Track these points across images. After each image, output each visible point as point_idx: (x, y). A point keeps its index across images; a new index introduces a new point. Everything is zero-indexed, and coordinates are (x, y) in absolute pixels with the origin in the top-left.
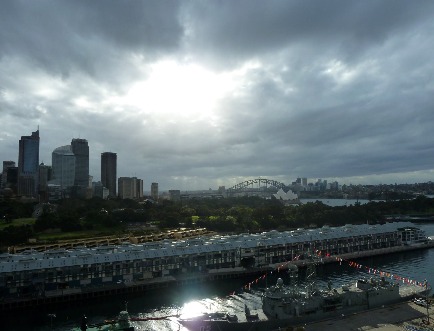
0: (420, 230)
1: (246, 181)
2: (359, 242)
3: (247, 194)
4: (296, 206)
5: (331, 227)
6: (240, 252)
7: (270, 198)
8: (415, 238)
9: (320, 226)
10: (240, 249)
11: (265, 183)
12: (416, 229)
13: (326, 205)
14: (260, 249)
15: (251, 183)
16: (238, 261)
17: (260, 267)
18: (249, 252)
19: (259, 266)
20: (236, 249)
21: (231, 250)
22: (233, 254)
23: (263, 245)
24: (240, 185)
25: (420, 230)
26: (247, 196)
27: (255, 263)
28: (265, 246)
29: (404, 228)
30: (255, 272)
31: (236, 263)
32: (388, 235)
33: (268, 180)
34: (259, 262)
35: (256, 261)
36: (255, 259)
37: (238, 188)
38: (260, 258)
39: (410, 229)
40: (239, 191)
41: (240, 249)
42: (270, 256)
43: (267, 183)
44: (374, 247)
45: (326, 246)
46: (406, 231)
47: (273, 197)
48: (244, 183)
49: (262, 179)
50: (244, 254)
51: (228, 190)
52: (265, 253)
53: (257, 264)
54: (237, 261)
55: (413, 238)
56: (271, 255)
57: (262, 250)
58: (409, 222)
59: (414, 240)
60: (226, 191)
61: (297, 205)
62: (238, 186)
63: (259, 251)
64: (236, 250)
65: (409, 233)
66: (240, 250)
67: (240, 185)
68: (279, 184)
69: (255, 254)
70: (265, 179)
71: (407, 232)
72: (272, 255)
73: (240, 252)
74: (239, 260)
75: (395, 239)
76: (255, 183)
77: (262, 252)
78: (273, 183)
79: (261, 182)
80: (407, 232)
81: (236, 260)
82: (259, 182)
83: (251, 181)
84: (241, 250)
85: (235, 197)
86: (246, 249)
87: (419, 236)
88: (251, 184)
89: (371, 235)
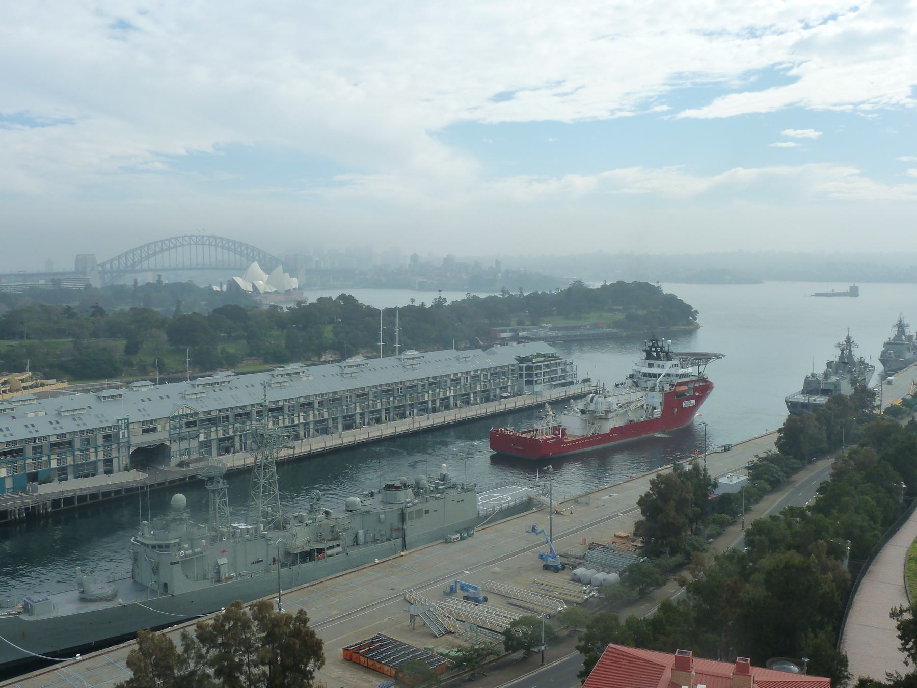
0: (562, 359)
1: (159, 241)
2: (430, 392)
3: (160, 276)
4: (288, 309)
5: (368, 358)
6: (126, 431)
7: (225, 288)
8: (552, 378)
9: (343, 358)
10: (129, 424)
11: (213, 245)
12: (556, 357)
13: (364, 305)
14: (183, 421)
15: (172, 245)
16: (121, 458)
17: (184, 468)
18: (154, 430)
19: (181, 464)
20: (114, 426)
21: (99, 429)
22: (107, 438)
23: (192, 412)
24: (141, 251)
25: (562, 359)
26: (159, 282)
27: (169, 457)
28: (196, 414)
29: (532, 355)
30: (170, 482)
31: (115, 463)
32: (495, 373)
33: (219, 238)
34: (182, 453)
35: (172, 454)
36: (170, 449)
37: (134, 258)
38: (185, 445)
39: (542, 359)
40: (138, 267)
41: (129, 424)
42: (212, 438)
43: (216, 245)
44: (463, 402)
45: (353, 405)
46: (534, 363)
47: (233, 285)
48: (153, 246)
49: (203, 237)
50: (141, 440)
51: (103, 265)
52: (198, 430)
53: (174, 461)
54: (118, 457)
55: (549, 378)
56: (213, 436)
57: (189, 424)
58: (542, 342)
59: (549, 382)
60: (100, 268)
61: (293, 305)
62: (134, 254)
63: (182, 427)
64: (117, 427)
65: (539, 368)
66: (127, 427)
67: (141, 251)
68: (249, 250)
69: (170, 434)
70: (213, 237)
71: (536, 365)
72: (217, 433)
73: (128, 432)
74: (126, 454)
75: (510, 381)
76: (183, 245)
77: (189, 429)
78: (233, 247)
79: (200, 242)
80: (536, 365)
81: (114, 454)
82: (196, 244)
83: (174, 241)
84: (131, 426)
85: (123, 286)
86: (143, 423)
87: (560, 373)
88: (173, 248)
89: (459, 375)
